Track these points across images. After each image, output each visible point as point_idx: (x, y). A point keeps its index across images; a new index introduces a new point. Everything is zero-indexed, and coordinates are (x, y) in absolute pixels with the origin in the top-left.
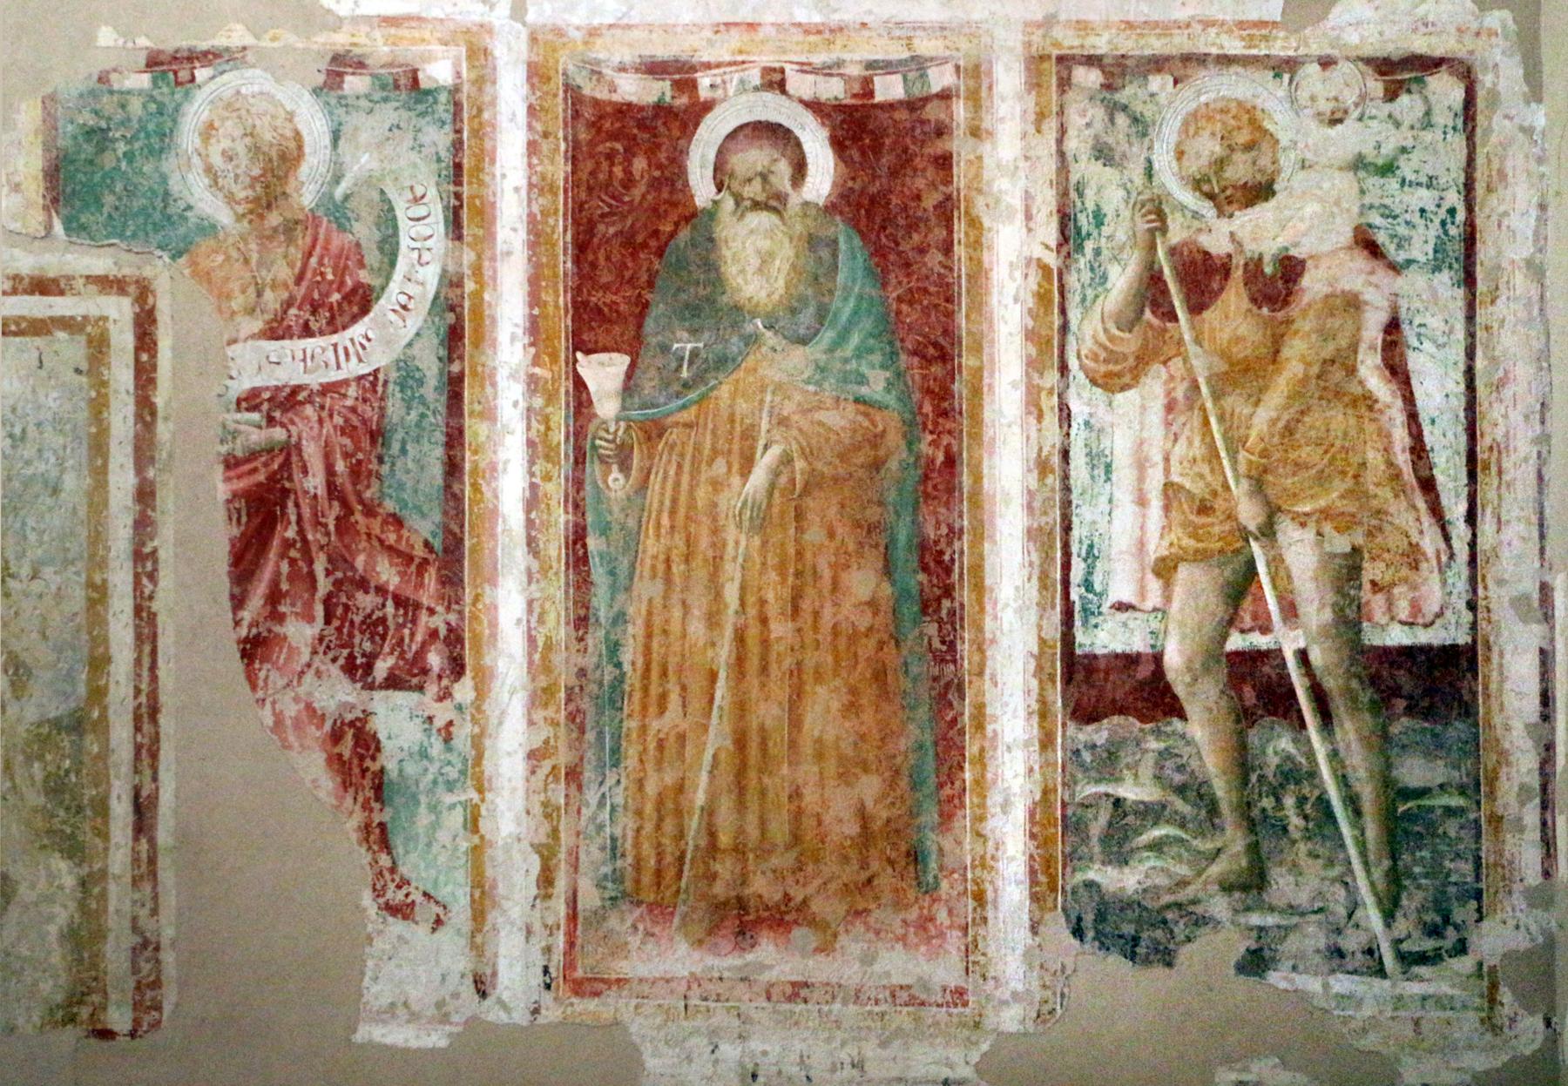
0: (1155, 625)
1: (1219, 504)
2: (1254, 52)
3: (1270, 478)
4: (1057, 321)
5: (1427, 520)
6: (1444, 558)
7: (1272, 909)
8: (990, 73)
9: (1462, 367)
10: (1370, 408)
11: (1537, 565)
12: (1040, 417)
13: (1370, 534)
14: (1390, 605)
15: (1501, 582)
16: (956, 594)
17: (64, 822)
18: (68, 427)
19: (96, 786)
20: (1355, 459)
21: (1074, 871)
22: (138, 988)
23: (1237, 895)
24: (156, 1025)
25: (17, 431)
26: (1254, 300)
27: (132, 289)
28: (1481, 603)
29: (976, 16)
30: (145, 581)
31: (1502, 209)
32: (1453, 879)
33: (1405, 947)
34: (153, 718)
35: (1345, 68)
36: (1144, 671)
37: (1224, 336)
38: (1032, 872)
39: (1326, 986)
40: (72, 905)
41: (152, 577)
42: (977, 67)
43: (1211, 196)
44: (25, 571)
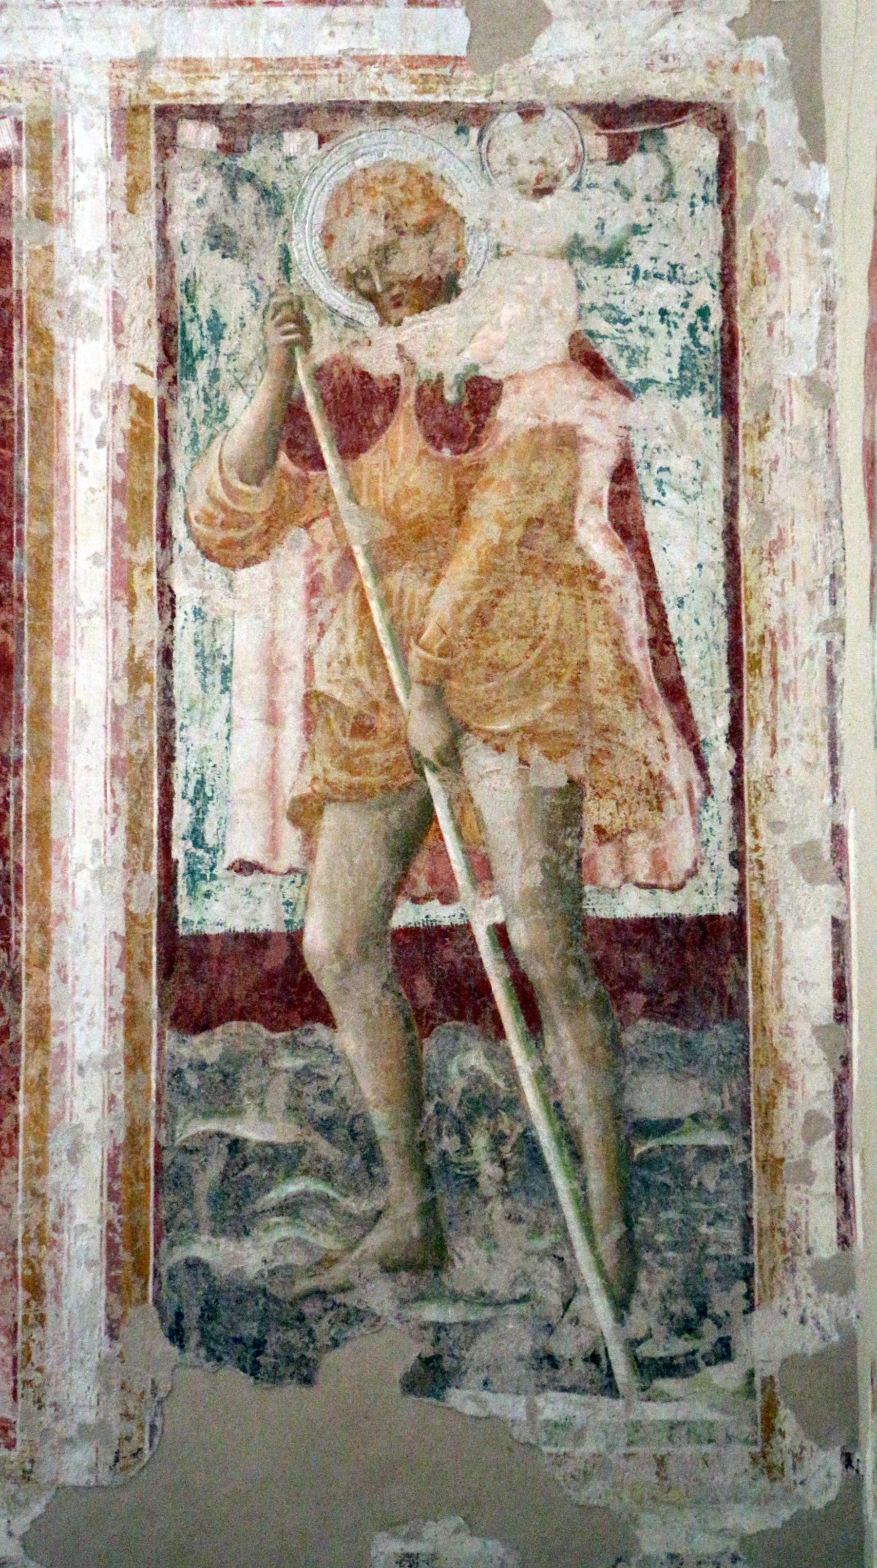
0: (290, 892)
1: (383, 722)
2: (429, 98)
3: (454, 684)
4: (156, 470)
5: (673, 740)
6: (698, 794)
7: (455, 1298)
8: (63, 130)
9: (720, 525)
10: (594, 586)
11: (828, 800)
12: (132, 604)
13: (594, 760)
14: (623, 860)
15: (777, 826)
16: (10, 853)
20: (574, 658)
21: (172, 1245)
23: (404, 1276)
26: (431, 438)
28: (750, 856)
29: (43, 54)
31: (771, 310)
32: (712, 1250)
33: (646, 1350)
35: (555, 119)
36: (275, 958)
37: (389, 489)
38: (111, 1247)
39: (532, 1411)
42: (45, 124)
43: (371, 297)
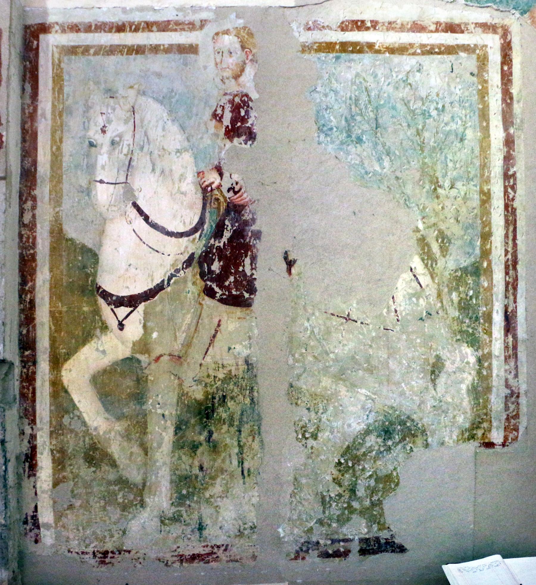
17: (468, 327)
18: (467, 105)
19: (486, 305)
22: (507, 419)
24: (515, 439)
25: (440, 106)
27: (500, 30)
30: (509, 190)
34: (515, 268)
40: (474, 373)
41: (513, 188)
44: (447, 184)
